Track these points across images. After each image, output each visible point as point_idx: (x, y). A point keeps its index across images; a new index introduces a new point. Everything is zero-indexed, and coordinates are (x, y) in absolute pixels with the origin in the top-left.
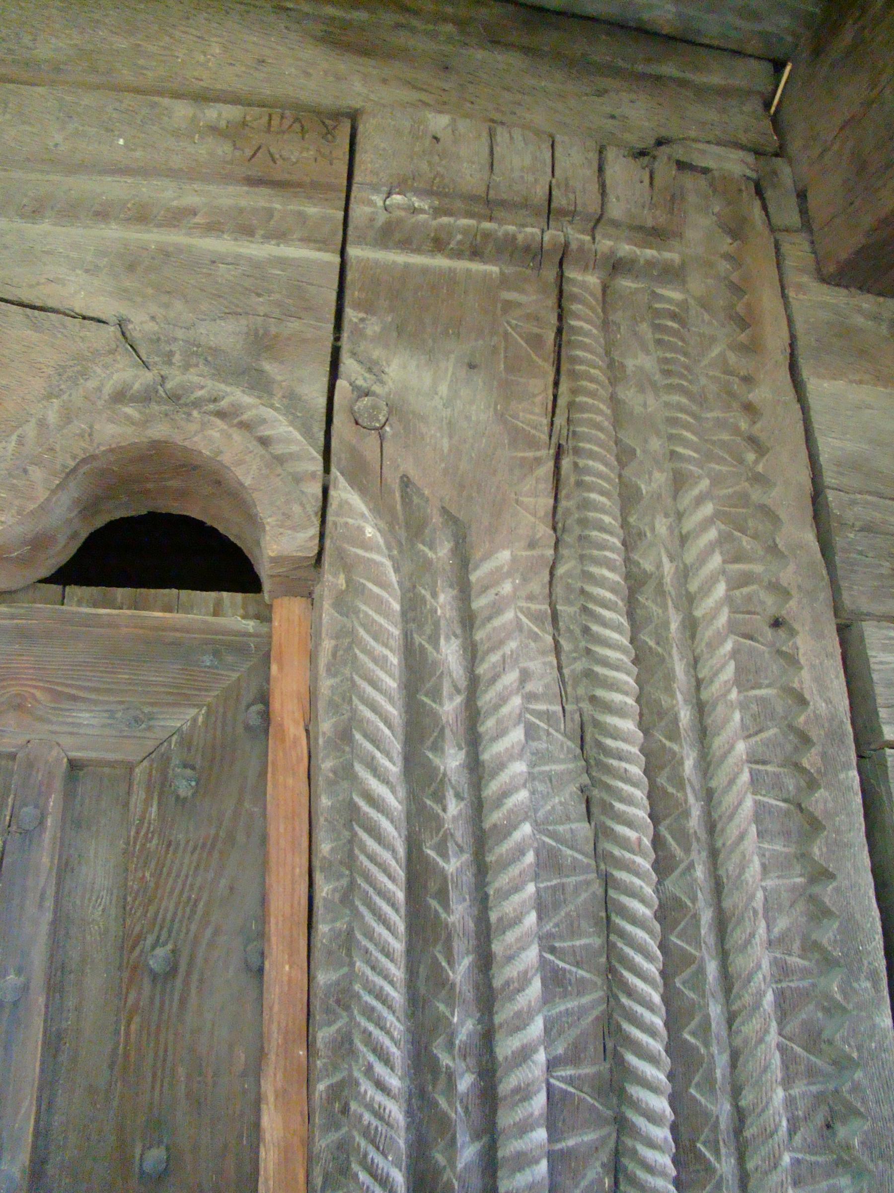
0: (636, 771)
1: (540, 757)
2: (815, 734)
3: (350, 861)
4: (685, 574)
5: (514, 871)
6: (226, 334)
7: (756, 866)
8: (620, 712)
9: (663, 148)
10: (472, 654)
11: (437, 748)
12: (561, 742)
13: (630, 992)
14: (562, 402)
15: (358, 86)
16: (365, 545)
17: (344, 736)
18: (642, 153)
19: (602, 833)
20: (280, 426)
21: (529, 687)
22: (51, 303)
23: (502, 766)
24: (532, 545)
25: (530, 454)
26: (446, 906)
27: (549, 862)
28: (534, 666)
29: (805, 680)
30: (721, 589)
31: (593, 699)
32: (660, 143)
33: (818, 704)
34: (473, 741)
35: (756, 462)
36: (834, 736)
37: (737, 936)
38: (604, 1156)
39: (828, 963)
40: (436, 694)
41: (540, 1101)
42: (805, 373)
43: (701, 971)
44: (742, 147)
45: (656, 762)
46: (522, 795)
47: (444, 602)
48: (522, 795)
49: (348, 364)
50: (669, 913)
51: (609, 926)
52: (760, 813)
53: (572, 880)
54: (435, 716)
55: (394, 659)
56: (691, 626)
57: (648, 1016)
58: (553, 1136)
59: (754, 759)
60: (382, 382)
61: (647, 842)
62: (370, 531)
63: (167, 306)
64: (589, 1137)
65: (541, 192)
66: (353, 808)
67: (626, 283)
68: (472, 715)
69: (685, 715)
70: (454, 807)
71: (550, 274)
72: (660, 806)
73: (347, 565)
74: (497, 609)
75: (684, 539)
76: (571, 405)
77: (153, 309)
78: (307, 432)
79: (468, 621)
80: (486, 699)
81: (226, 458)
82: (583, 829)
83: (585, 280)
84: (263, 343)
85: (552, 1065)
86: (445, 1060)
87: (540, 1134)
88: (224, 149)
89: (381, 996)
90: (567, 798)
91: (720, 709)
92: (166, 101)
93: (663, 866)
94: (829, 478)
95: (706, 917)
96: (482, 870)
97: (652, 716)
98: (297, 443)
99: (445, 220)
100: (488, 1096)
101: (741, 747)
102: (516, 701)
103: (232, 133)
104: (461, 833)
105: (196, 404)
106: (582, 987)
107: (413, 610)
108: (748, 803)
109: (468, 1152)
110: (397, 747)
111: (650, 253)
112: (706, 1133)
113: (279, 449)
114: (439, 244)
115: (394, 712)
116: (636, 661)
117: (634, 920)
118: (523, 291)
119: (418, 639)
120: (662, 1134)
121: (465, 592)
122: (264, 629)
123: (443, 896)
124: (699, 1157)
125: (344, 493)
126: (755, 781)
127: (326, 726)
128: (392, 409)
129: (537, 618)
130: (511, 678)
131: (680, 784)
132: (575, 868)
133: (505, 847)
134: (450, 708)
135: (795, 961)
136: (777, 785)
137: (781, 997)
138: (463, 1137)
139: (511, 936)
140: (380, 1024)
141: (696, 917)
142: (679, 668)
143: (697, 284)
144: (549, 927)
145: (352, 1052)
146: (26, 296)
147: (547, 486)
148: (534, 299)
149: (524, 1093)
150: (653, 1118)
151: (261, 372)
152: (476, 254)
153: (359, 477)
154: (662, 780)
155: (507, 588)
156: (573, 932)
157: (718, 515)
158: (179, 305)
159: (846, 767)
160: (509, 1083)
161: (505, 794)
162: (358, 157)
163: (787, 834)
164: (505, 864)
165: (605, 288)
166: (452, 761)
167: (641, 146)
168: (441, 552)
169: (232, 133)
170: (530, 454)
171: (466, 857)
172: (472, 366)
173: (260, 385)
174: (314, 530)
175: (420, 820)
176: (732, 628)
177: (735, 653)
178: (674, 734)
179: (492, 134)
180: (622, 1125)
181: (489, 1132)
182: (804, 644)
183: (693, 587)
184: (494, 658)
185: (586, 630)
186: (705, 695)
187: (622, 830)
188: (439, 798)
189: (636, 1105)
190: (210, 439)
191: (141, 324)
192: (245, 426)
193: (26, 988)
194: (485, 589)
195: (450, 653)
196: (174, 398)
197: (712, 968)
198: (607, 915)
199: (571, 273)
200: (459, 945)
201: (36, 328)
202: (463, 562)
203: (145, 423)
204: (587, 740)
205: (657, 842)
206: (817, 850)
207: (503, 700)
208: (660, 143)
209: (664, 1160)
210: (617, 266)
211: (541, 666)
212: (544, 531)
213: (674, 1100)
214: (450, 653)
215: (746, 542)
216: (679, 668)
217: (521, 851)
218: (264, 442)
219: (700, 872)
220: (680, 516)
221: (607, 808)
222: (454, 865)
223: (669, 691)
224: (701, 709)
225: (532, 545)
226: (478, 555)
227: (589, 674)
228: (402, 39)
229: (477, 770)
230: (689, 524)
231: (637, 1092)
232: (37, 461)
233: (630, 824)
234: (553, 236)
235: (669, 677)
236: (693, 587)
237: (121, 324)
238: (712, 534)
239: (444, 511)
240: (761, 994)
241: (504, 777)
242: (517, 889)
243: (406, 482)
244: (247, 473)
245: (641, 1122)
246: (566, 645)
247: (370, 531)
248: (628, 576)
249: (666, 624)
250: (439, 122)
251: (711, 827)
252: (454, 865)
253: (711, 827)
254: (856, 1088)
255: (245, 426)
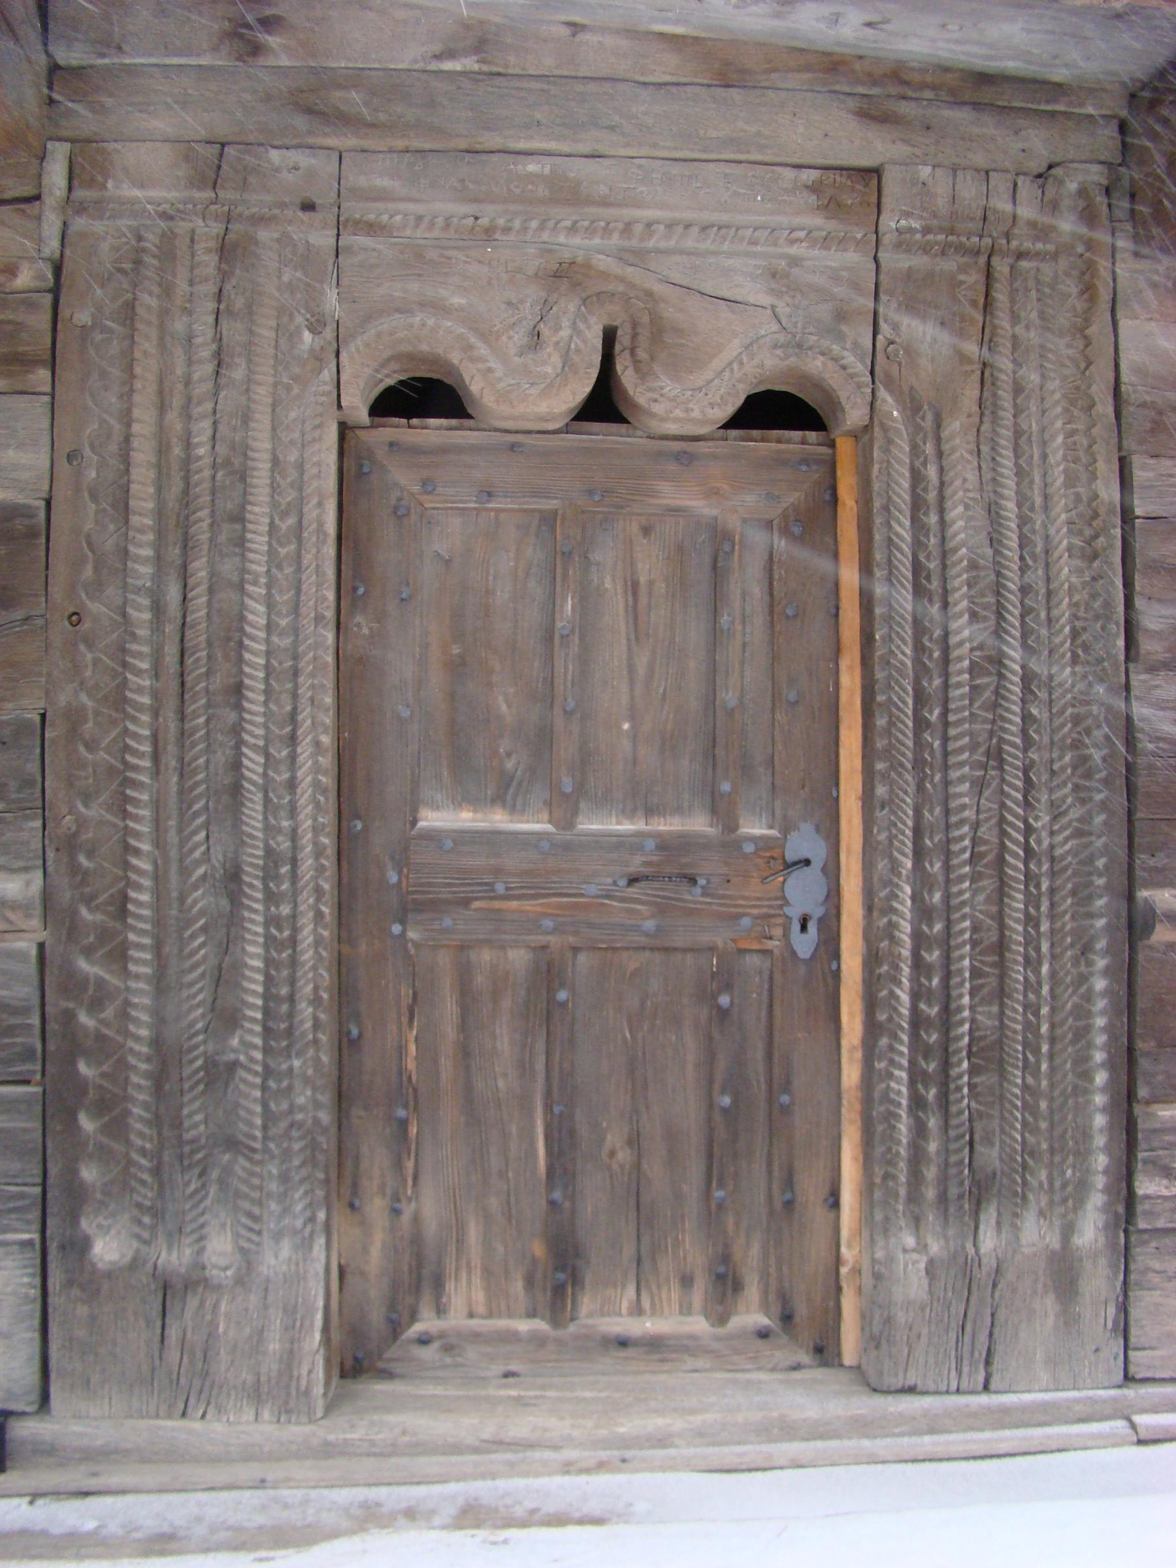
0: (1013, 526)
1: (970, 518)
2: (1102, 511)
3: (890, 562)
4: (1043, 430)
5: (958, 568)
6: (824, 311)
7: (1066, 570)
8: (1007, 499)
9: (1053, 171)
10: (941, 470)
11: (926, 514)
12: (979, 512)
13: (1005, 620)
14: (986, 339)
15: (879, 145)
16: (894, 420)
17: (886, 508)
18: (1040, 176)
19: (997, 552)
20: (849, 358)
21: (967, 486)
22: (739, 299)
23: (953, 522)
24: (969, 416)
25: (968, 368)
26: (929, 581)
27: (973, 566)
28: (969, 476)
29: (1099, 486)
30: (1060, 439)
31: (995, 492)
32: (1050, 167)
33: (1104, 494)
34: (942, 511)
35: (1087, 368)
36: (1111, 511)
37: (1055, 600)
38: (992, 688)
39: (1097, 617)
40: (925, 490)
41: (966, 663)
42: (1119, 315)
43: (1038, 615)
44: (1101, 163)
45: (1023, 521)
46: (963, 536)
47: (929, 448)
48: (963, 536)
49: (884, 326)
50: (1025, 590)
51: (998, 593)
52: (1069, 549)
53: (982, 574)
54: (925, 501)
55: (907, 474)
56: (1044, 457)
57: (1014, 632)
58: (972, 678)
59: (1070, 522)
60: (898, 335)
61: (1016, 558)
62: (895, 413)
63: (793, 297)
64: (986, 680)
65: (979, 214)
66: (890, 540)
67: (1024, 264)
68: (941, 498)
69: (1038, 500)
70: (933, 540)
71: (982, 260)
72: (1024, 541)
73: (885, 429)
74: (953, 450)
75: (1044, 412)
76: (990, 341)
77: (787, 298)
78: (863, 362)
79: (940, 454)
80: (948, 492)
81: (827, 376)
82: (989, 552)
83: (1001, 267)
84: (841, 316)
85: (972, 650)
86: (928, 644)
87: (967, 676)
88: (812, 199)
89: (902, 617)
90: (983, 537)
91: (1056, 499)
92: (778, 169)
93: (1024, 569)
94: (1124, 378)
95: (1043, 591)
96: (944, 567)
97: (1022, 500)
98: (861, 368)
99: (930, 237)
100: (946, 660)
101: (1063, 516)
102: (961, 493)
103: (814, 188)
104: (936, 553)
105: (810, 348)
106: (985, 618)
107: (915, 448)
108: (1065, 542)
109: (937, 682)
110: (908, 514)
111: (1039, 246)
112: (1036, 682)
113: (850, 371)
114: (926, 249)
115: (907, 497)
116: (1016, 475)
117: (1010, 591)
118: (966, 272)
119: (917, 464)
120: (1017, 679)
121: (938, 441)
122: (829, 451)
123: (928, 578)
124: (1032, 692)
125: (882, 393)
126: (1070, 531)
127: (877, 504)
128: (907, 351)
129: (971, 453)
130: (958, 482)
131: (1034, 532)
132: (985, 568)
133: (955, 558)
134: (932, 496)
135: (1081, 614)
136: (1080, 533)
137: (1073, 629)
138: (935, 676)
139: (957, 595)
140: (902, 628)
141: (1037, 594)
142: (1037, 478)
143: (1063, 263)
144: (972, 593)
145: (891, 640)
146: (727, 295)
147: (978, 385)
148: (974, 278)
149: (960, 659)
150: (1013, 672)
151: (840, 332)
152: (943, 253)
153: (889, 384)
154: (1025, 530)
155: (958, 441)
156: (984, 596)
157: (1064, 396)
158: (799, 296)
159: (1114, 527)
160: (955, 654)
161: (955, 535)
162: (884, 200)
163: (1083, 557)
164: (954, 564)
165: (1012, 267)
166: (933, 519)
167: (1036, 171)
168: (928, 423)
169: (814, 188)
170: (968, 368)
171: (937, 562)
172: (942, 324)
173: (840, 337)
174: (867, 410)
175: (918, 545)
176: (1065, 458)
177: (1065, 471)
178: (1032, 509)
179: (955, 176)
180: (1001, 676)
181: (946, 675)
182: (1101, 465)
183: (1047, 436)
184: (952, 474)
185: (994, 459)
186: (1050, 491)
187: (1006, 552)
188: (927, 536)
189: (1005, 667)
190: (816, 365)
191: (783, 310)
192: (835, 360)
193: (733, 622)
194: (948, 440)
195: (932, 472)
196: (799, 346)
197: (1043, 615)
198: (998, 589)
199: (995, 261)
200: (936, 598)
201: (733, 312)
202: (938, 426)
203: (787, 357)
204: (993, 512)
205: (1022, 558)
206: (1096, 564)
207: (955, 493)
208: (1050, 167)
209: (1017, 690)
210: (1021, 255)
211: (972, 476)
212: (975, 408)
213: (1023, 667)
214: (932, 472)
215: (1076, 412)
216: (1037, 478)
217: (961, 561)
218: (844, 368)
219: (1040, 572)
220: (1043, 399)
221: (1000, 542)
222: (933, 565)
223: (1031, 488)
224: (1046, 497)
225: (969, 416)
226: (944, 424)
227: (994, 479)
228: (904, 108)
229: (942, 522)
230: (1047, 404)
231: (1007, 662)
232: (739, 381)
233: (1010, 549)
234: (987, 241)
235: (1032, 482)
236: (1047, 436)
237: (773, 307)
238: (1059, 409)
239: (929, 404)
240: (1063, 626)
241: (955, 527)
242: (959, 576)
243: (912, 388)
244: (833, 379)
245: (1008, 675)
246: (984, 466)
247: (895, 413)
248: (1016, 432)
249: (1032, 457)
250: (925, 171)
251: (1047, 552)
252: (933, 565)
253: (1047, 552)
254: (1104, 670)
255: (835, 360)
